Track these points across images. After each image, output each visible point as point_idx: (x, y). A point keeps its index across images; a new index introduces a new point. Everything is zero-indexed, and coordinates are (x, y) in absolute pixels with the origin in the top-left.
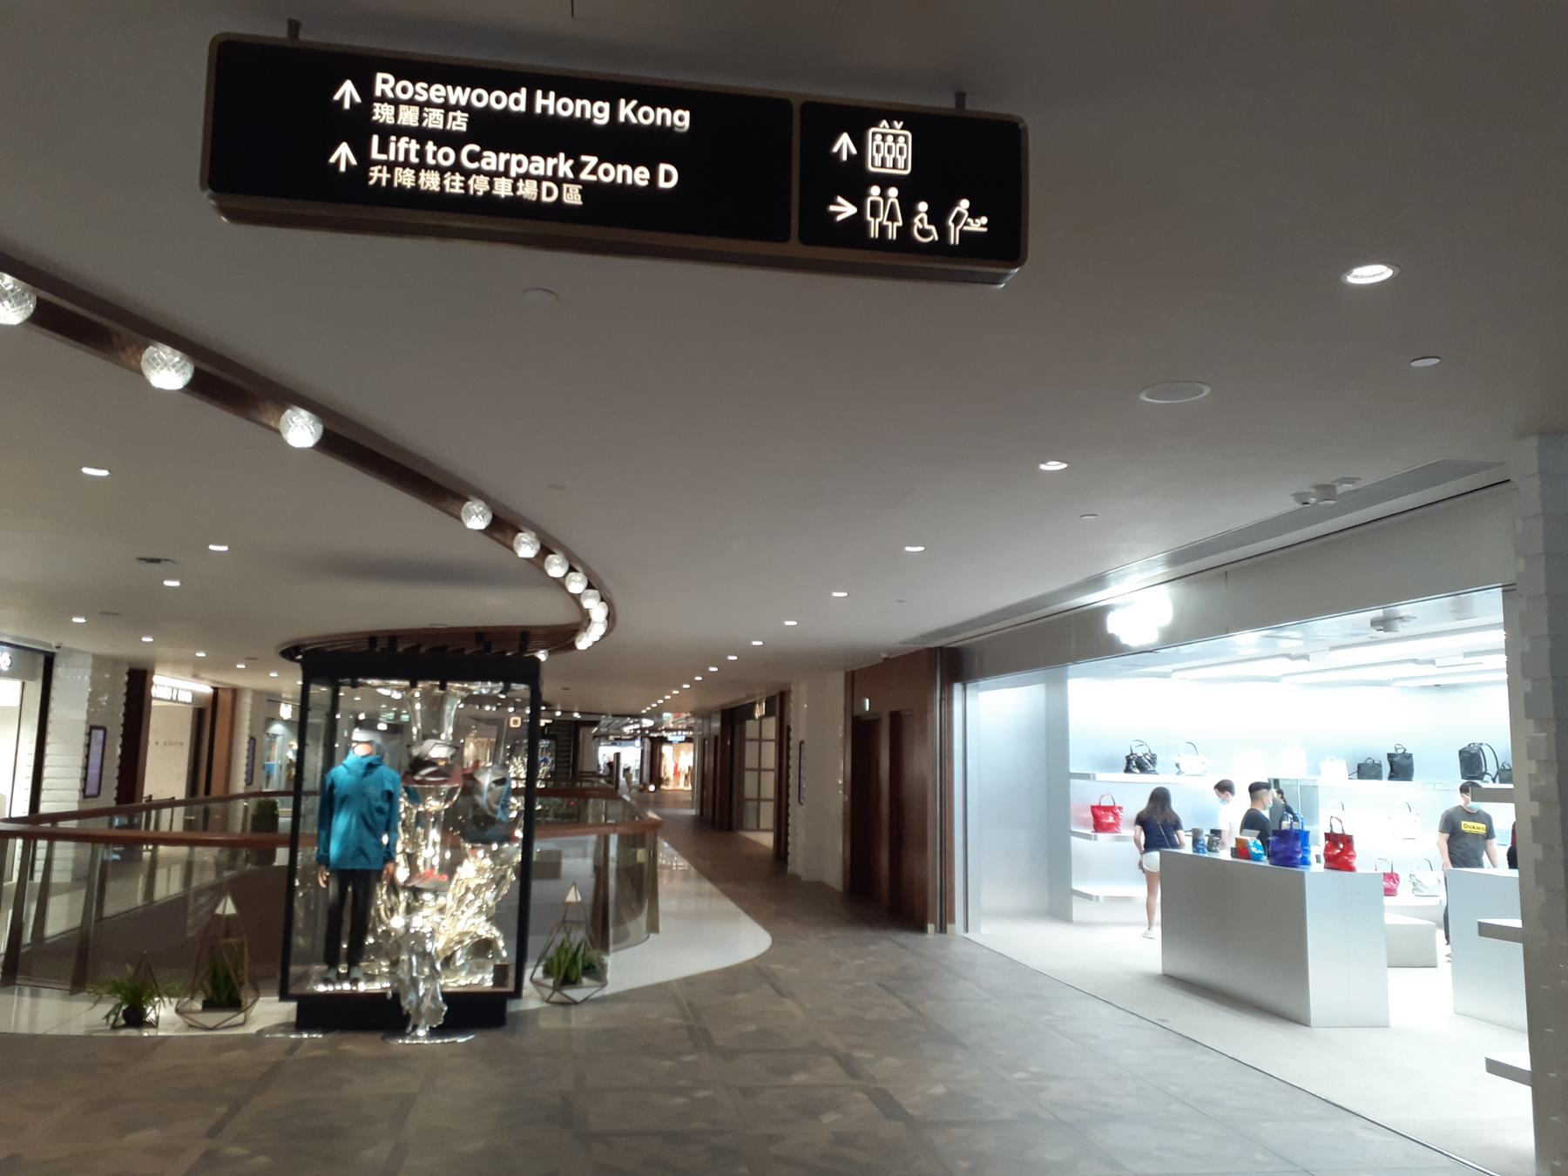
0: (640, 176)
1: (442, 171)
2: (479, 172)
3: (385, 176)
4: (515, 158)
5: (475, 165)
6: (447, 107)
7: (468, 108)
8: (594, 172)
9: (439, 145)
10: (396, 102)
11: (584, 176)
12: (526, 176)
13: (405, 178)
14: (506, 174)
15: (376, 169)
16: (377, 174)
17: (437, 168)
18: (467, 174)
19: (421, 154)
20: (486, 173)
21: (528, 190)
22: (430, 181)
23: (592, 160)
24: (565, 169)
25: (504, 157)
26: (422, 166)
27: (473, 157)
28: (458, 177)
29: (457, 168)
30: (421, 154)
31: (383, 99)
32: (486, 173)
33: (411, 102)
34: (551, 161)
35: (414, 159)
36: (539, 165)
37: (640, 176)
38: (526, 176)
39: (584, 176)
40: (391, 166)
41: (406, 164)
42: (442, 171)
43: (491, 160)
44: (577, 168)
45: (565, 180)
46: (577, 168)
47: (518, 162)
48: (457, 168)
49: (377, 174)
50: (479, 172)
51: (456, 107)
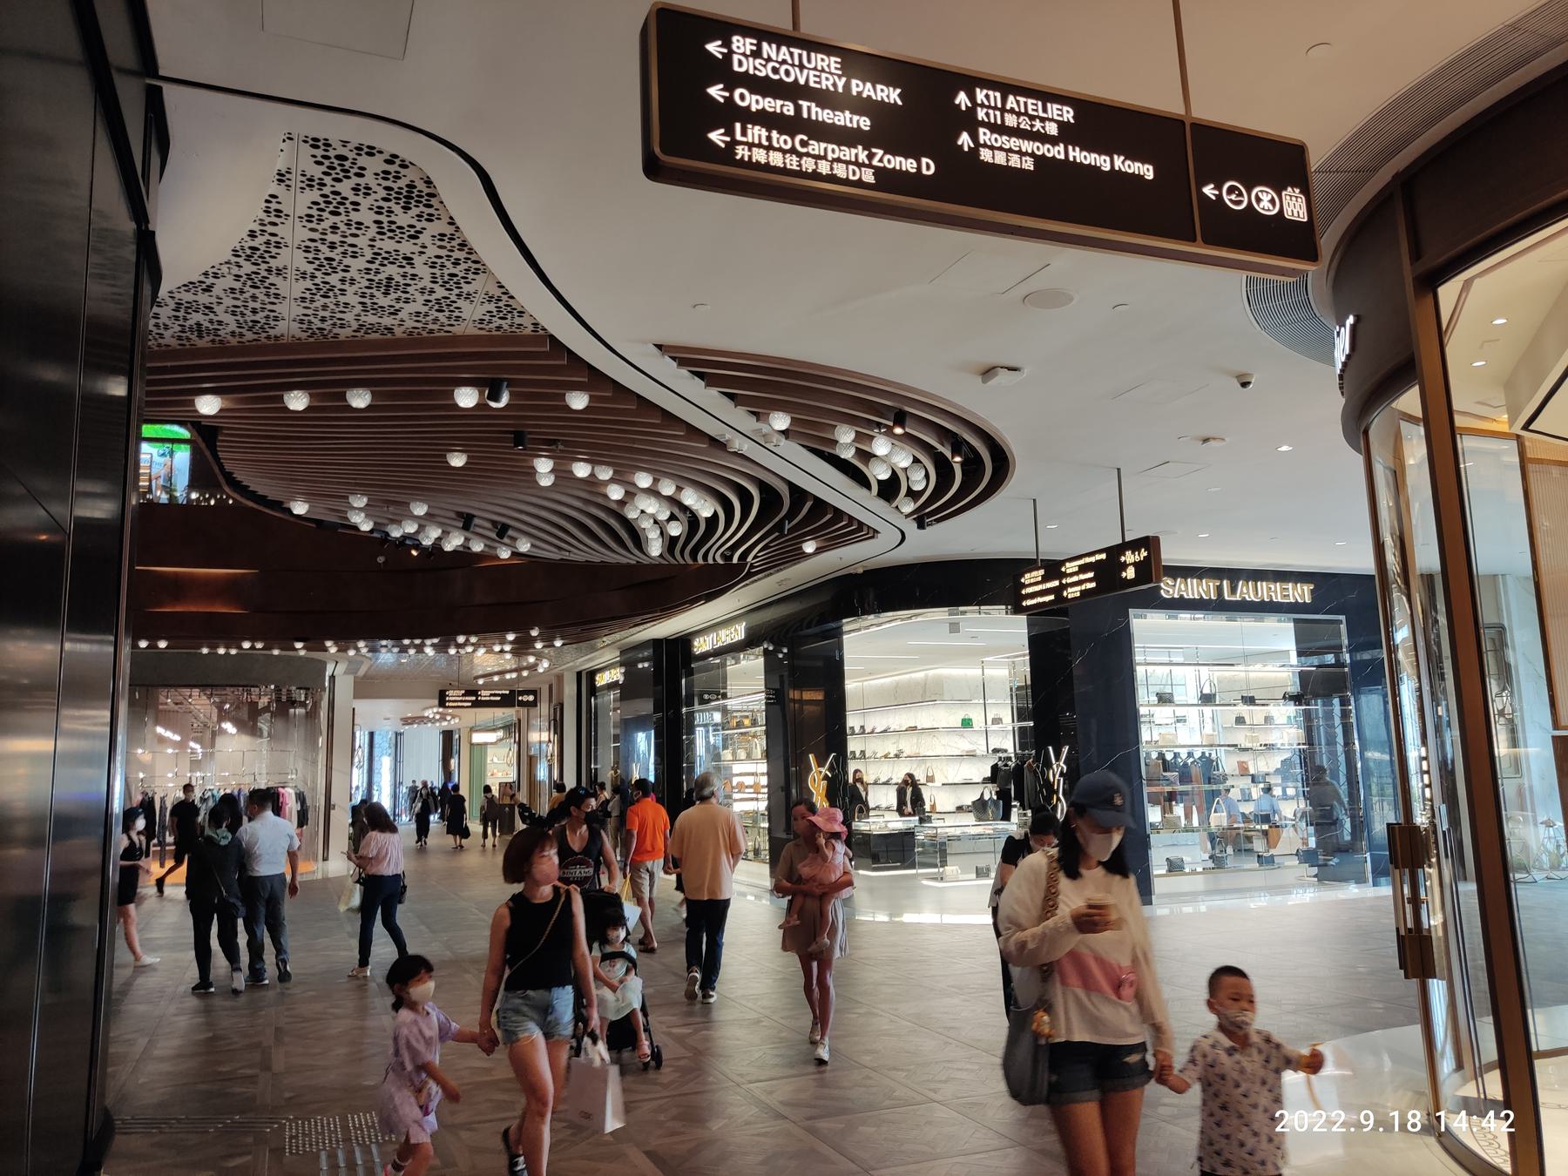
0: (909, 165)
1: (784, 152)
2: (808, 155)
3: (747, 153)
4: (830, 147)
5: (804, 150)
6: (1021, 153)
7: (1032, 155)
8: (881, 160)
9: (781, 133)
10: (992, 148)
11: (875, 162)
12: (838, 160)
13: (759, 156)
14: (824, 158)
15: (740, 147)
16: (741, 152)
17: (780, 150)
18: (800, 155)
19: (769, 138)
20: (814, 157)
21: (840, 171)
22: (776, 159)
23: (880, 152)
24: (863, 157)
25: (823, 145)
26: (770, 148)
27: (804, 144)
28: (794, 158)
29: (793, 151)
30: (769, 138)
31: (985, 145)
32: (814, 157)
33: (1001, 149)
34: (854, 151)
35: (765, 143)
36: (847, 153)
37: (909, 165)
38: (838, 160)
39: (875, 162)
40: (751, 145)
41: (760, 146)
42: (784, 152)
43: (816, 147)
44: (871, 156)
45: (863, 165)
46: (871, 156)
47: (833, 151)
48: (793, 151)
49: (741, 152)
50: (808, 155)
51: (1026, 154)
